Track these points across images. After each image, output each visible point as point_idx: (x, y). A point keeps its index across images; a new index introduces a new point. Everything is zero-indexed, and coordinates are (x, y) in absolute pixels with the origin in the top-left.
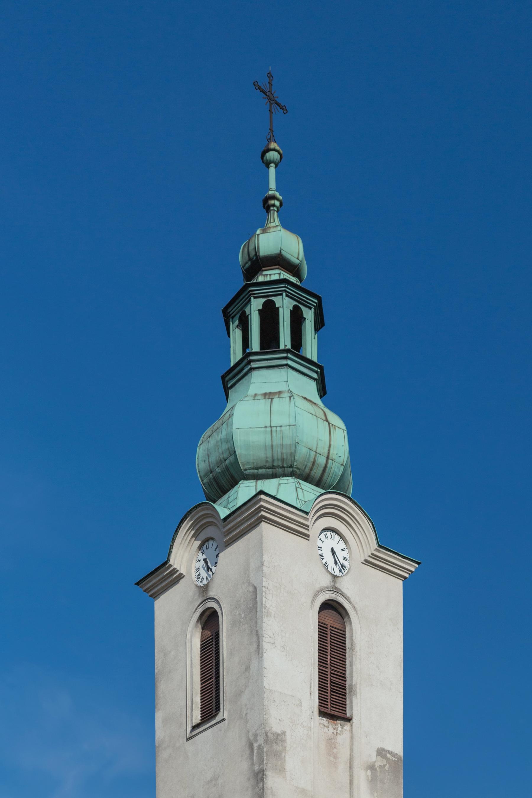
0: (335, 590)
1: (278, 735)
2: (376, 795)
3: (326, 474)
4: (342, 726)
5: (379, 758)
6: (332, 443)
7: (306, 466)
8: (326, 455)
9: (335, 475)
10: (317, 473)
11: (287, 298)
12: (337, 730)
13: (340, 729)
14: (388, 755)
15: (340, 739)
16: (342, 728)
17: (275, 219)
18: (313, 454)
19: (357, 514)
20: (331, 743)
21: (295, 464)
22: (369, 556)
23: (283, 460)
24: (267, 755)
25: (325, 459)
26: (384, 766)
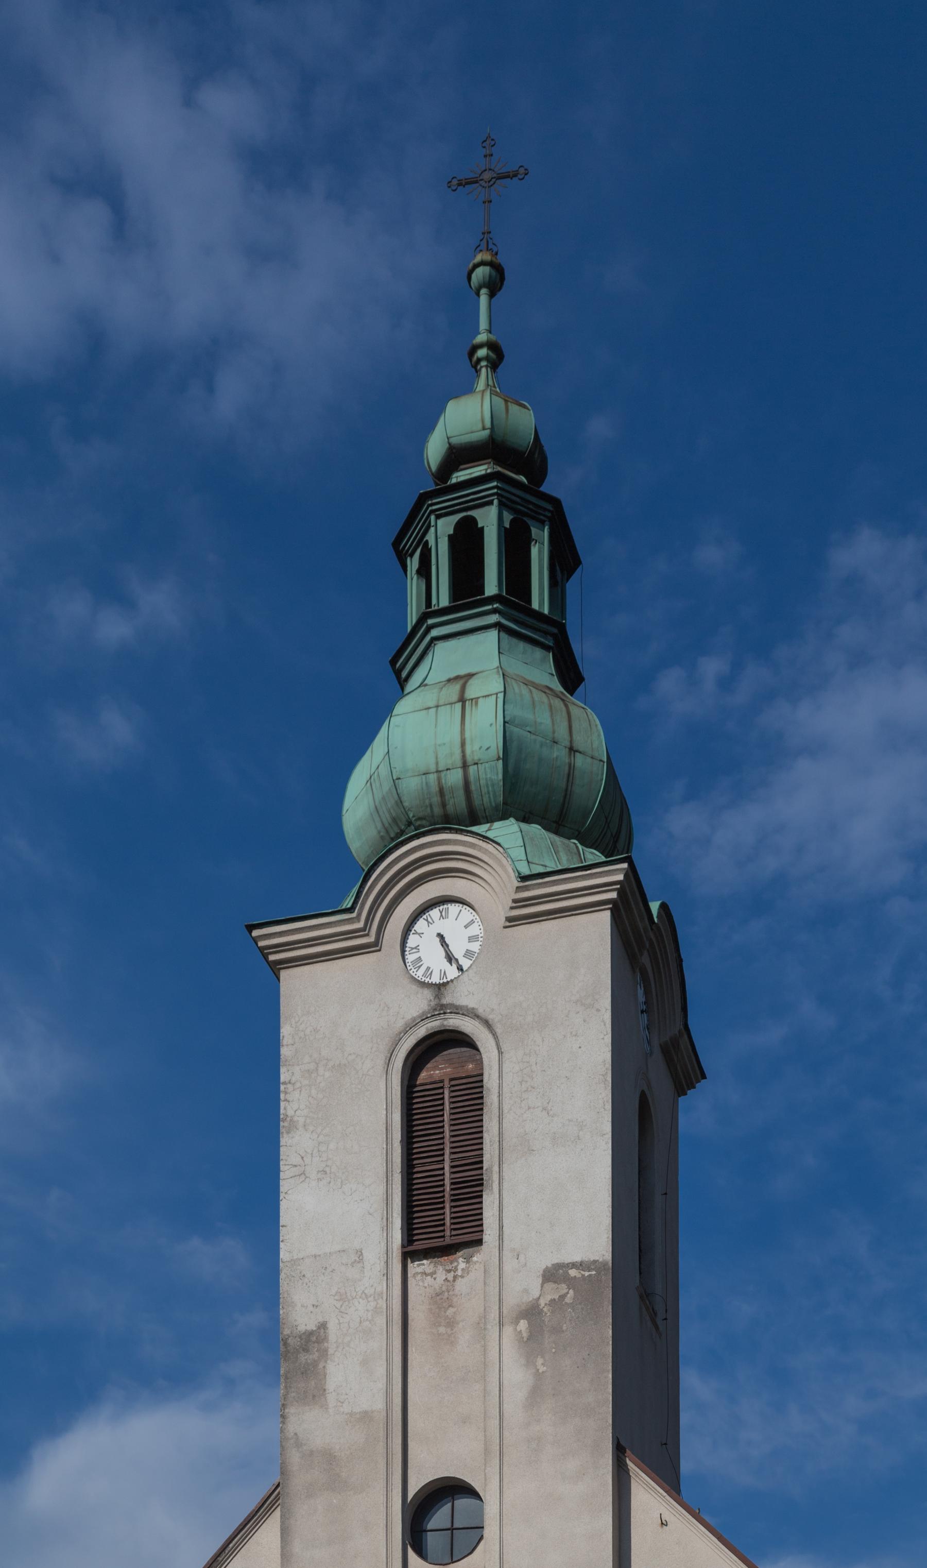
0: (441, 1009)
1: (311, 1333)
2: (540, 1361)
3: (475, 796)
4: (468, 1259)
5: (550, 1286)
6: (467, 735)
7: (431, 806)
9: (493, 785)
10: (457, 803)
11: (440, 522)
12: (456, 1269)
13: (462, 1265)
14: (573, 1273)
15: (462, 1286)
16: (468, 1262)
18: (432, 778)
19: (472, 846)
20: (442, 1301)
21: (411, 815)
22: (512, 908)
23: (395, 820)
24: (286, 1378)
25: (460, 771)
26: (562, 1297)
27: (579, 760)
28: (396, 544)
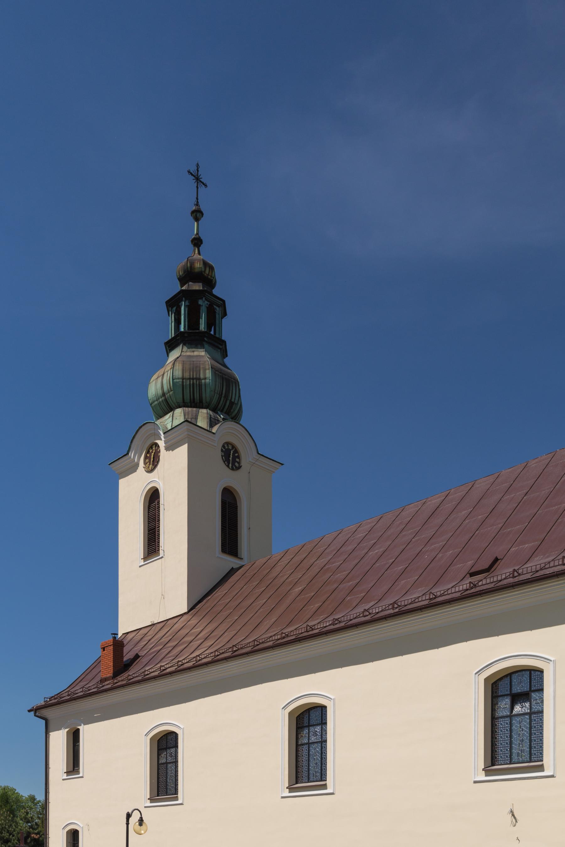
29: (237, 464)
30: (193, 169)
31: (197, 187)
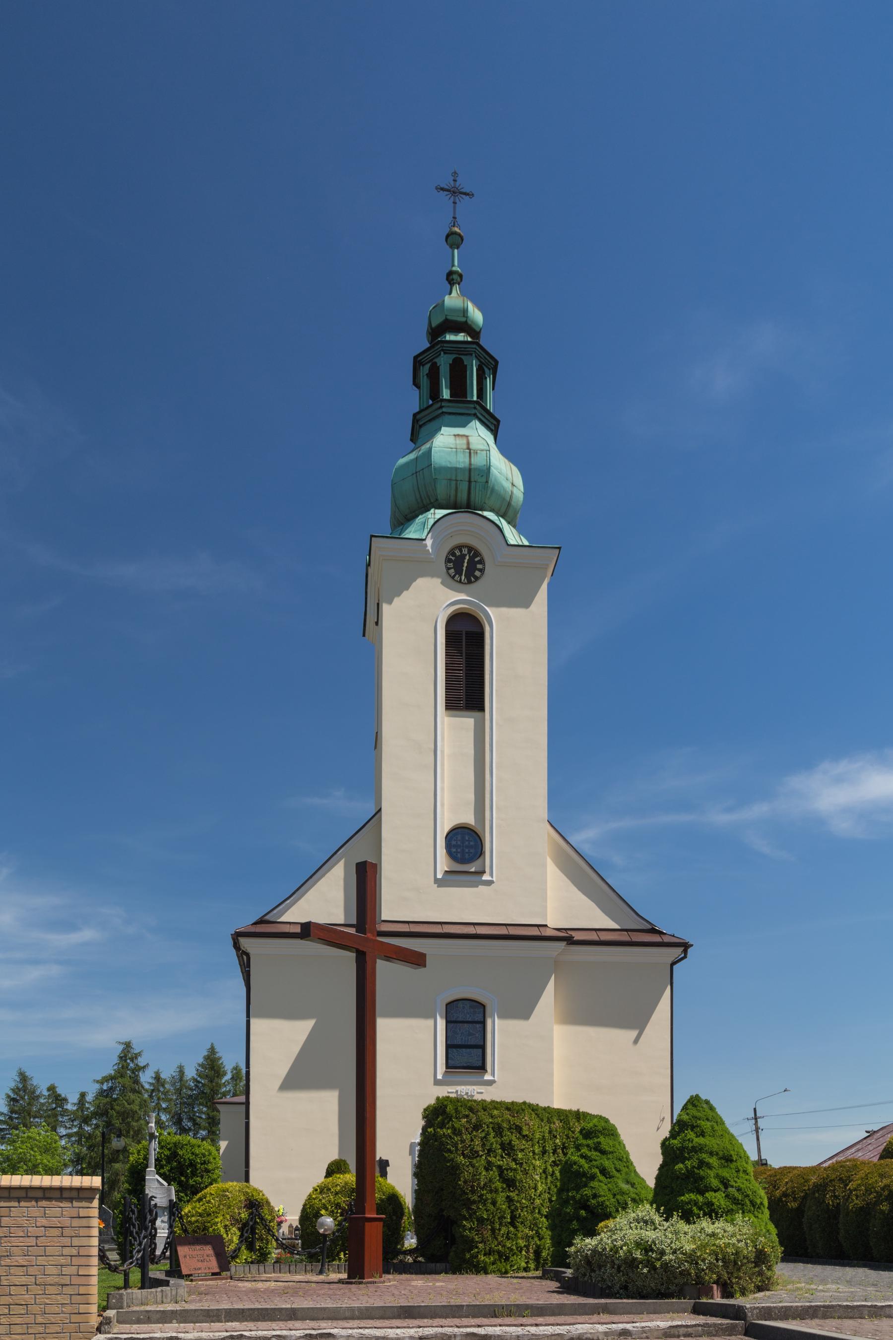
8: (467, 479)
17: (456, 290)
25: (467, 483)
27: (515, 490)
28: (415, 358)
29: (477, 573)
30: (447, 182)
31: (455, 203)
